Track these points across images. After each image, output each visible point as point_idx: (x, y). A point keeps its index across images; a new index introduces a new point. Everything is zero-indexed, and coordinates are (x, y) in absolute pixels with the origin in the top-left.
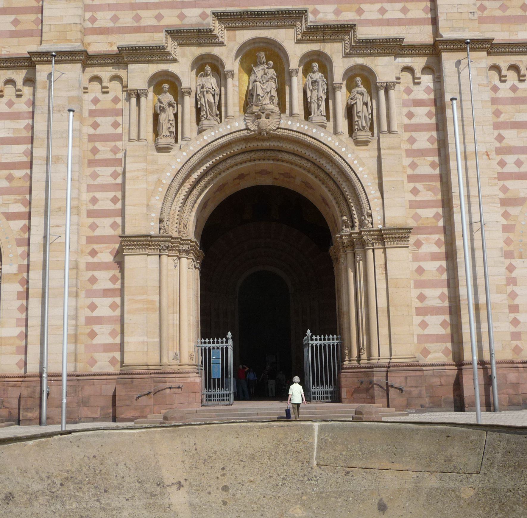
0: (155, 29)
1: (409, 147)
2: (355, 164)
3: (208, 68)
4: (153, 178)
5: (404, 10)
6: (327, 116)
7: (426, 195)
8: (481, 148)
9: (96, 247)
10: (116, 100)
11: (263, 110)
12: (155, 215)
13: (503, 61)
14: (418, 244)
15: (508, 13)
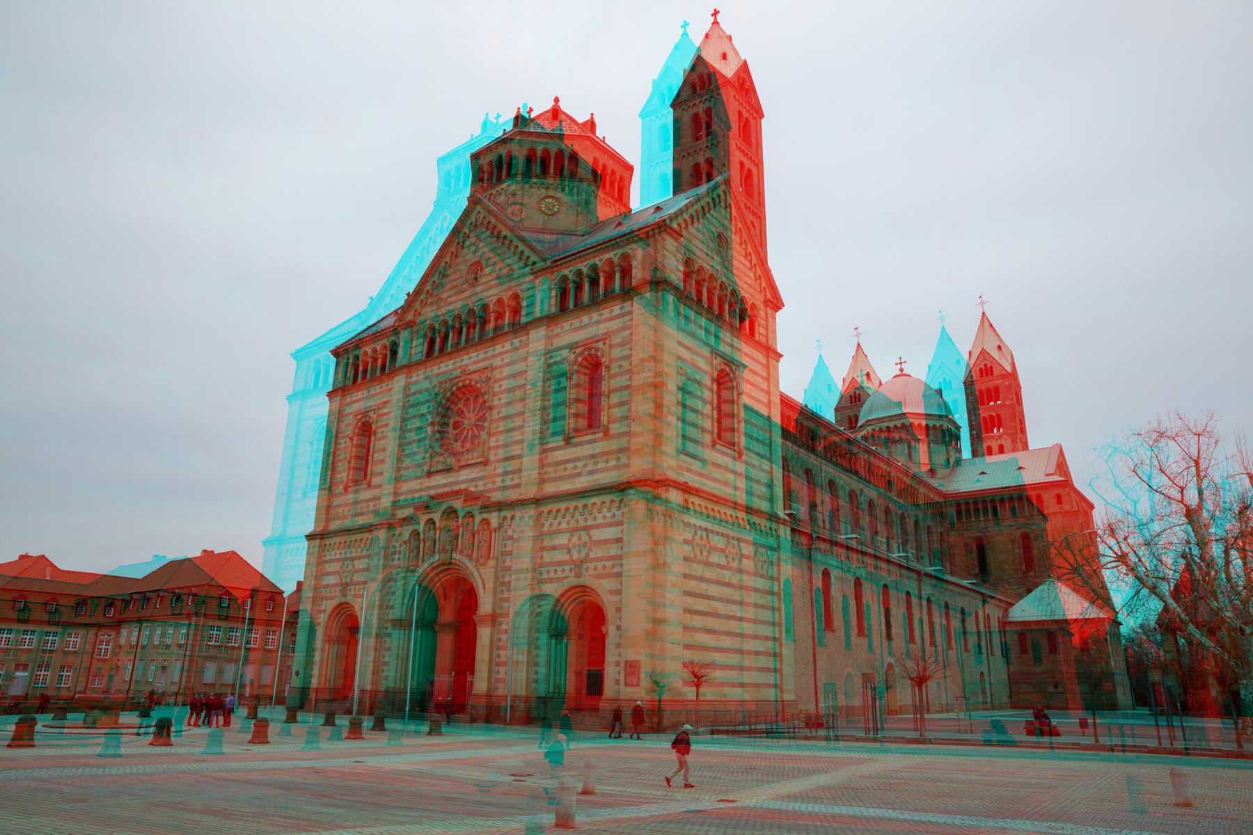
6: (473, 550)
10: (400, 546)
12: (404, 609)
13: (545, 509)
14: (501, 624)
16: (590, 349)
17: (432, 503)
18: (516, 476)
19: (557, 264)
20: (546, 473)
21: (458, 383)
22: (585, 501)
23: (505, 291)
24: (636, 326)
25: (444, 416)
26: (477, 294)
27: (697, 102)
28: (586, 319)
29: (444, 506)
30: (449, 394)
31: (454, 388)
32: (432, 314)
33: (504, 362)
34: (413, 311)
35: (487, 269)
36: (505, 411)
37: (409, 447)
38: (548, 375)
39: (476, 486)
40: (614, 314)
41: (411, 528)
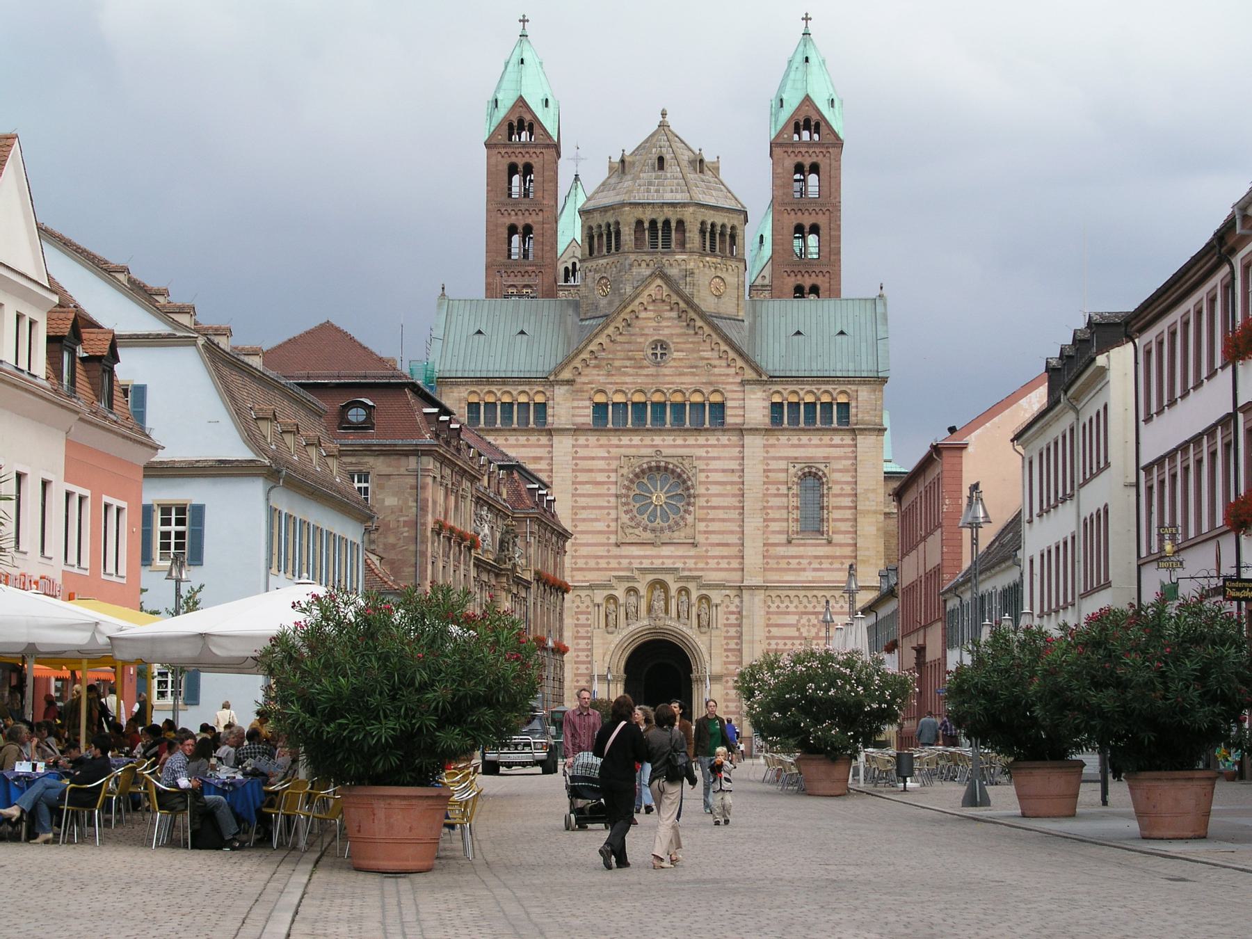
0: (606, 569)
1: (726, 634)
2: (699, 643)
3: (632, 593)
4: (606, 646)
5: (729, 563)
6: (688, 619)
7: (732, 659)
8: (757, 638)
9: (579, 678)
10: (588, 607)
11: (657, 617)
12: (607, 665)
13: (773, 594)
14: (727, 682)
15: (780, 566)
16: (811, 467)
17: (636, 574)
18: (731, 561)
19: (773, 379)
20: (767, 563)
21: (650, 462)
22: (815, 592)
23: (703, 383)
24: (861, 461)
25: (628, 488)
26: (667, 375)
27: (803, 150)
28: (805, 439)
29: (650, 577)
30: (637, 470)
31: (645, 466)
32: (602, 379)
33: (709, 455)
34: (571, 367)
35: (675, 353)
36: (715, 502)
37: (582, 511)
38: (766, 480)
39: (685, 563)
40: (833, 443)
41: (606, 593)
